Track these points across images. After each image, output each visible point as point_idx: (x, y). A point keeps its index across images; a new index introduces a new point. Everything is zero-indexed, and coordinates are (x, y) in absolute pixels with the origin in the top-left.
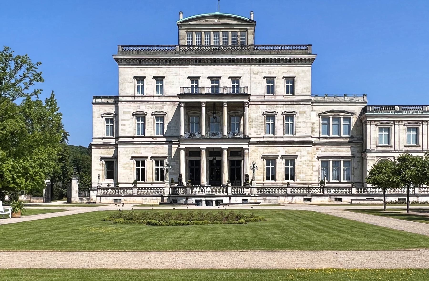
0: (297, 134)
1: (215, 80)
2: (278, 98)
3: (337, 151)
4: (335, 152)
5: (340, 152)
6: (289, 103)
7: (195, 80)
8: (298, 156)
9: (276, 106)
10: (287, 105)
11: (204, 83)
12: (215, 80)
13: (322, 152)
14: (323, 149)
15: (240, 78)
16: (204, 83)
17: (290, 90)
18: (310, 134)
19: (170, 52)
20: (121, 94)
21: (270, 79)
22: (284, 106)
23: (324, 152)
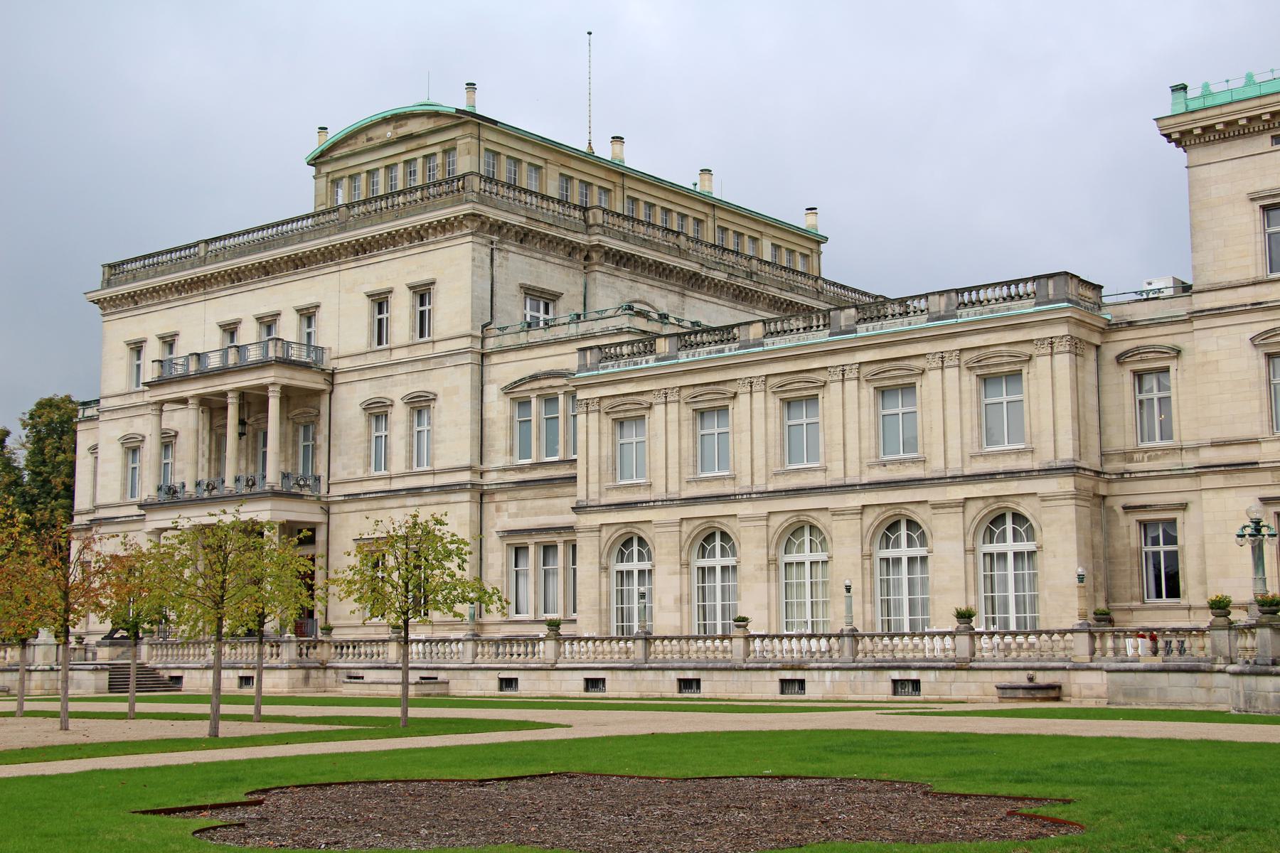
0: (439, 465)
1: (268, 322)
2: (399, 355)
3: (550, 513)
4: (543, 514)
5: (556, 513)
6: (420, 366)
7: (230, 329)
9: (390, 379)
10: (415, 375)
11: (249, 334)
12: (268, 322)
13: (510, 516)
14: (512, 507)
15: (317, 307)
16: (249, 334)
17: (423, 324)
19: (188, 263)
20: (106, 392)
21: (380, 301)
22: (410, 377)
23: (516, 515)
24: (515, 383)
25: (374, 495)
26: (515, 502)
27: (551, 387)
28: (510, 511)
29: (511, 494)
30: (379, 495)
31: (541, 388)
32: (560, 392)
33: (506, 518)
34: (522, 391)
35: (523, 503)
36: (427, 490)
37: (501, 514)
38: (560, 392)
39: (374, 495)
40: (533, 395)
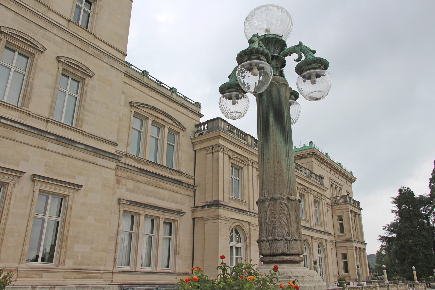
0: (85, 128)
5: (159, 198)
8: (81, 186)
18: (113, 139)
24: (143, 104)
25: (9, 123)
26: (132, 181)
27: (163, 120)
28: (128, 187)
29: (133, 175)
30: (17, 125)
31: (157, 117)
32: (167, 126)
33: (124, 190)
34: (142, 111)
35: (138, 184)
36: (80, 146)
37: (120, 186)
38: (167, 126)
39: (9, 123)
40: (151, 119)
